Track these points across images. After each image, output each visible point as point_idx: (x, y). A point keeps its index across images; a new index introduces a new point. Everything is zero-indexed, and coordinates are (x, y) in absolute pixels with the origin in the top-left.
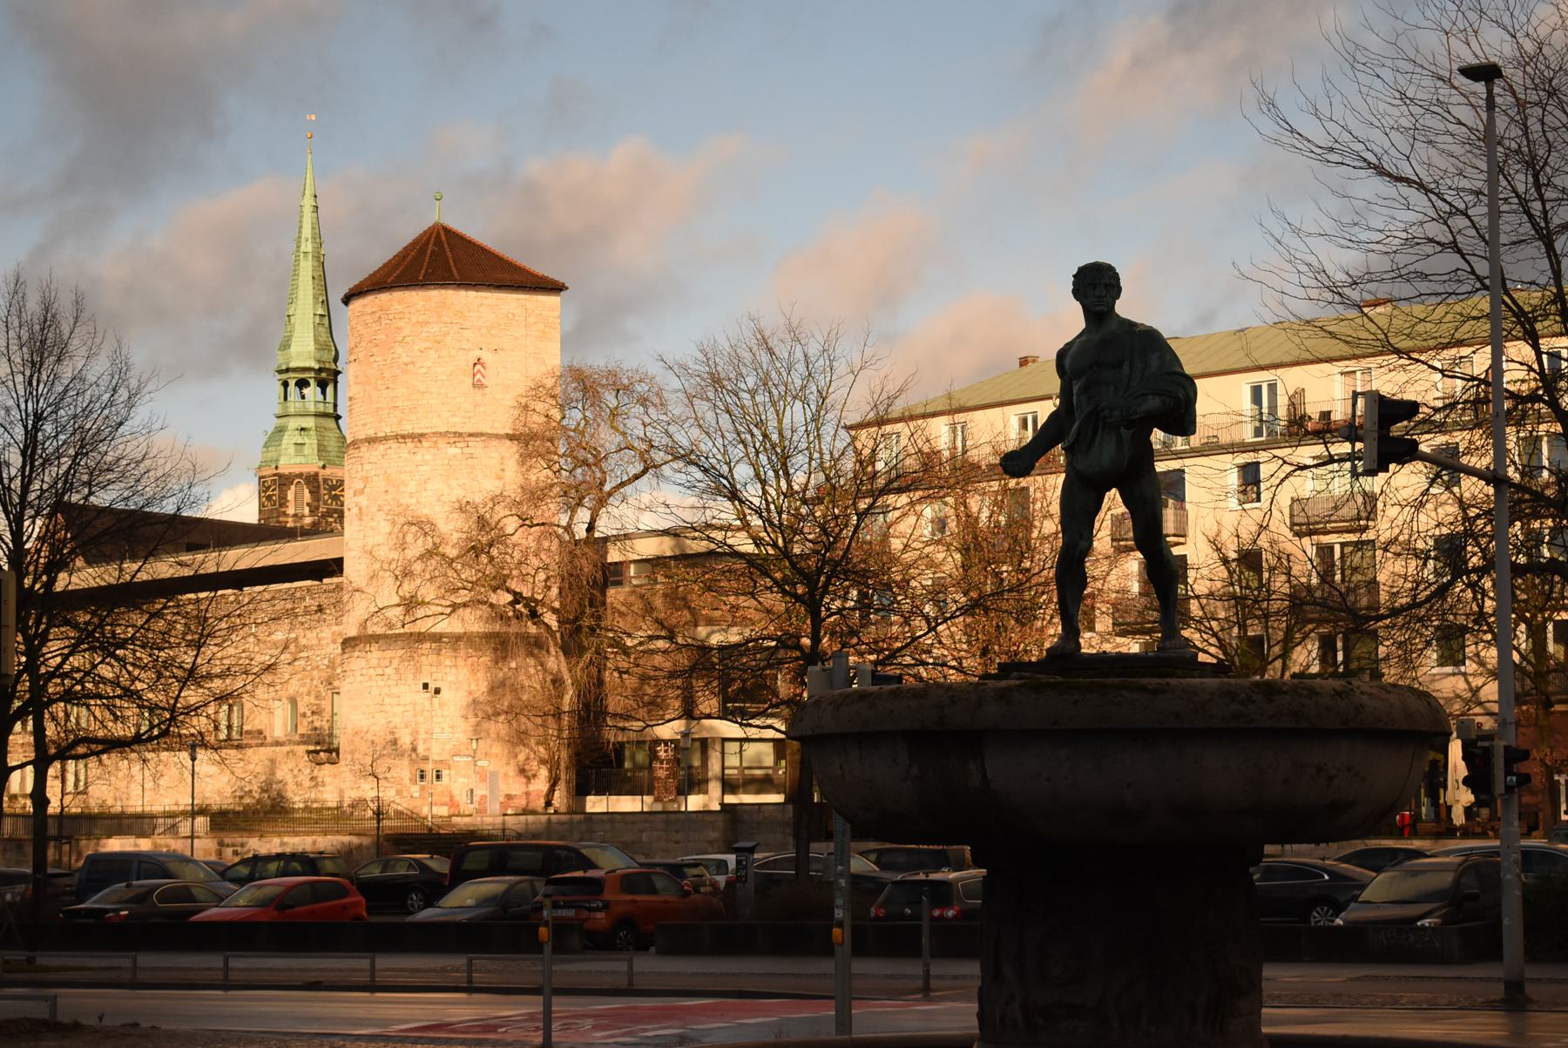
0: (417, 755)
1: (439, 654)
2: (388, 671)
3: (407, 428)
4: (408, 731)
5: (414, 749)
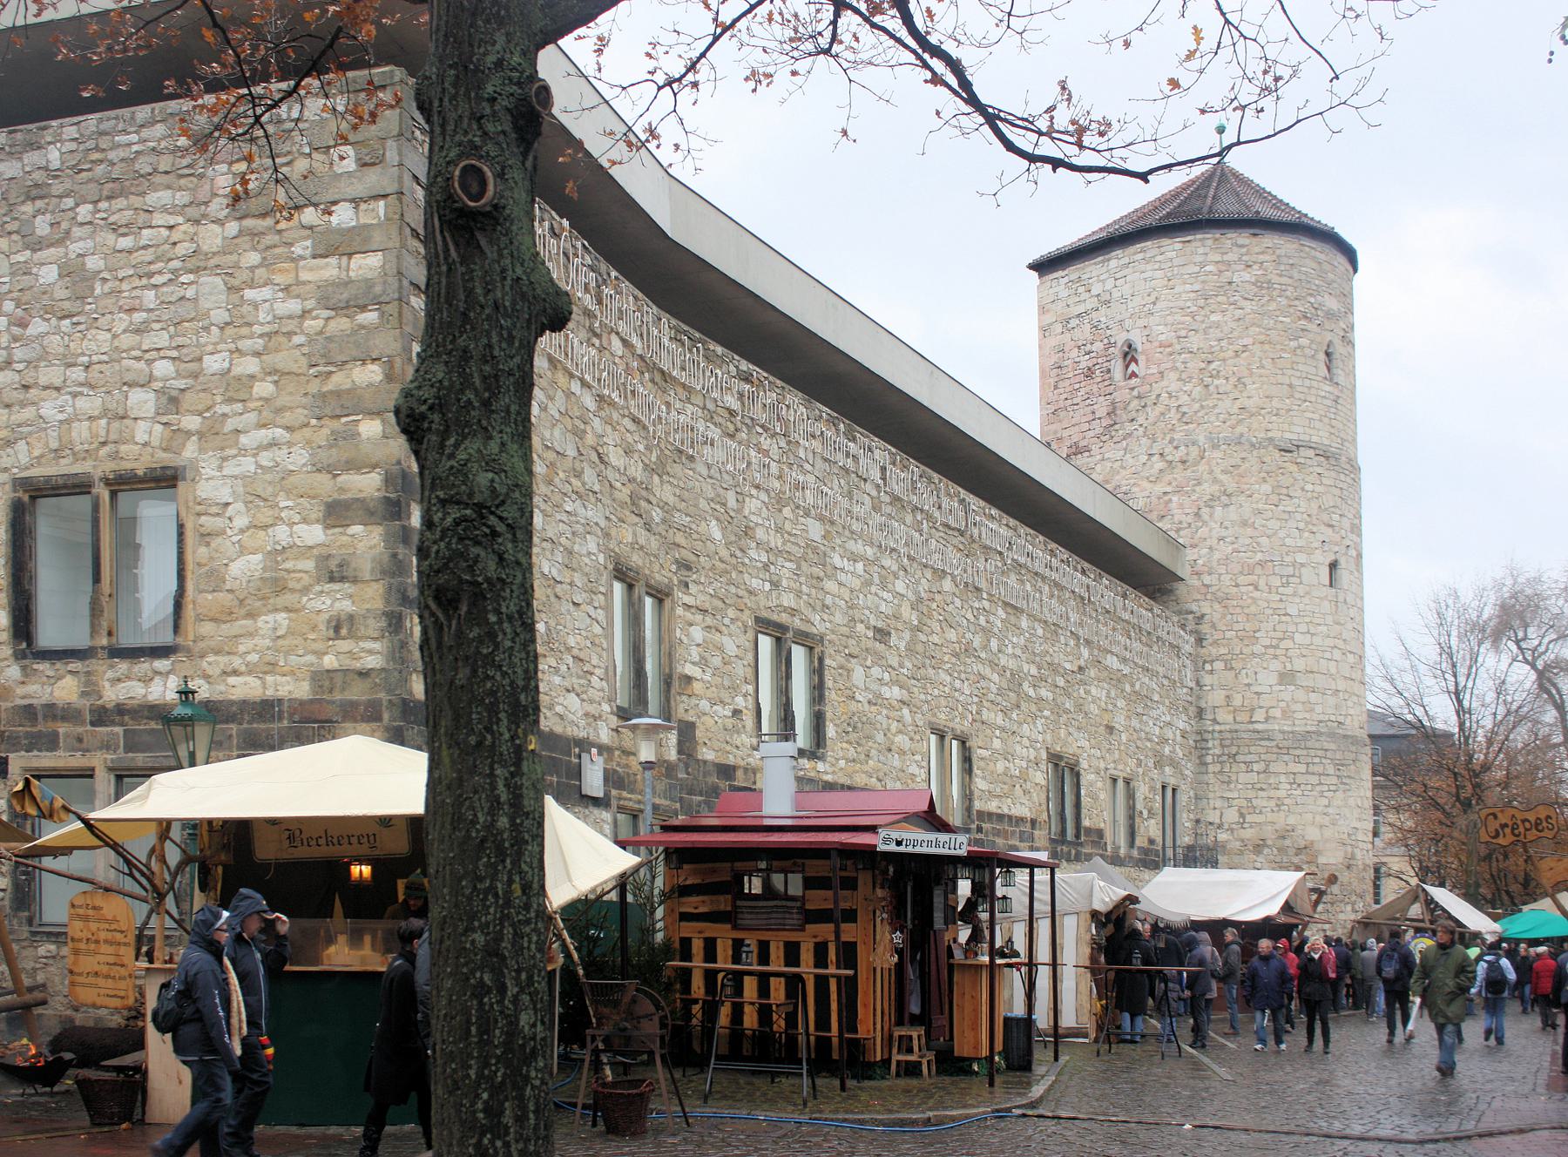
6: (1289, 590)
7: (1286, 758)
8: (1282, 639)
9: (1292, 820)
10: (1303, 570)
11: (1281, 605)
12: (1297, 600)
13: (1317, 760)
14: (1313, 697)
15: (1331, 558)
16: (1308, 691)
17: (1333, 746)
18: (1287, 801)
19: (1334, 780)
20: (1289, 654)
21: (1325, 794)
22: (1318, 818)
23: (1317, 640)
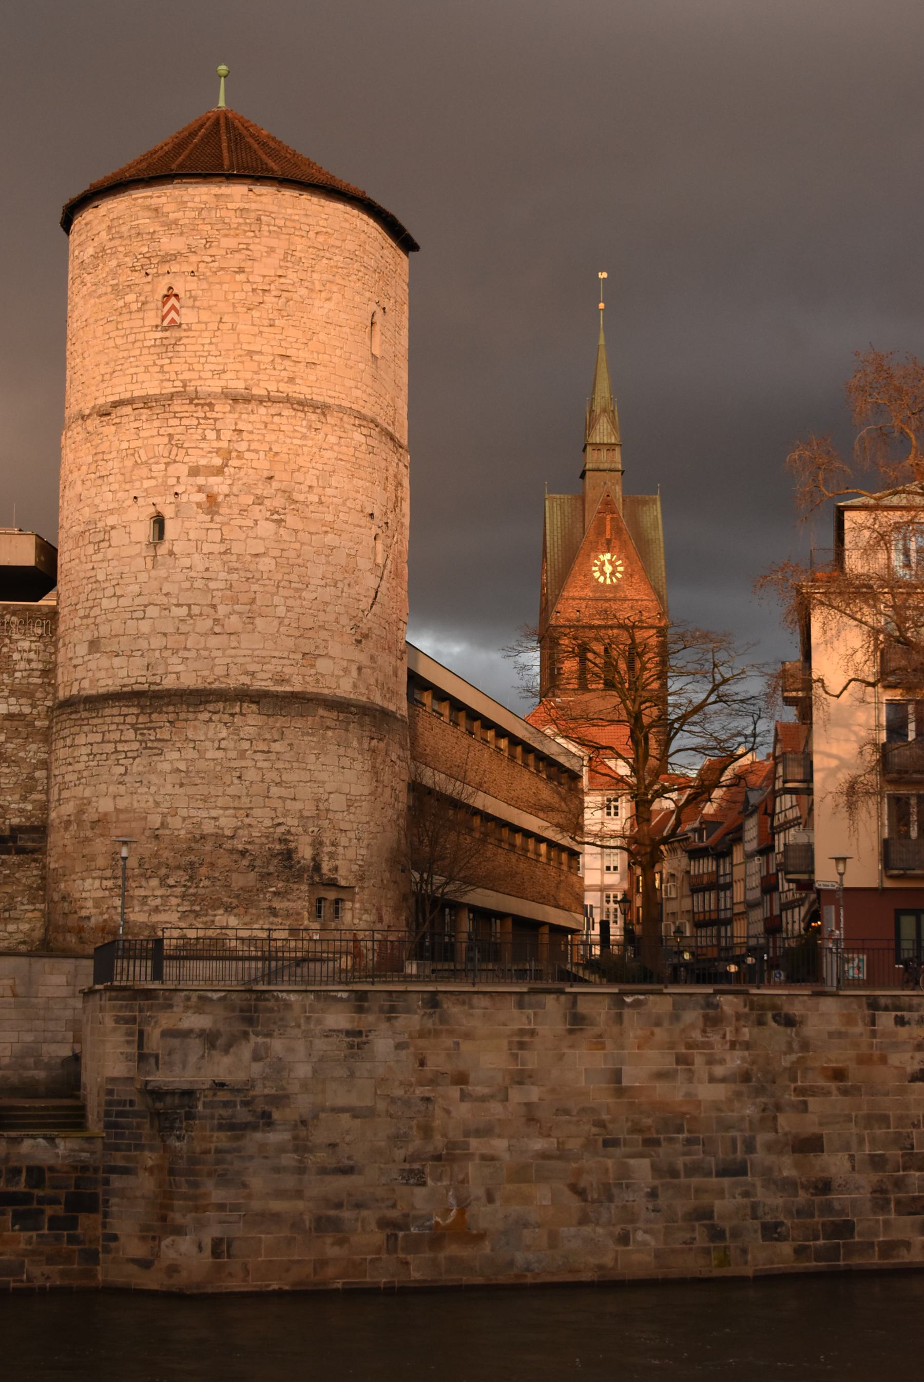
0: (321, 875)
1: (347, 730)
2: (276, 747)
3: (301, 390)
4: (308, 839)
5: (317, 868)
6: (100, 556)
7: (86, 728)
8: (91, 608)
9: (88, 793)
10: (113, 532)
11: (93, 573)
12: (105, 564)
13: (113, 727)
14: (117, 662)
15: (152, 510)
16: (109, 658)
17: (135, 711)
18: (85, 774)
19: (135, 746)
20: (97, 622)
21: (121, 762)
22: (112, 789)
23: (123, 602)
